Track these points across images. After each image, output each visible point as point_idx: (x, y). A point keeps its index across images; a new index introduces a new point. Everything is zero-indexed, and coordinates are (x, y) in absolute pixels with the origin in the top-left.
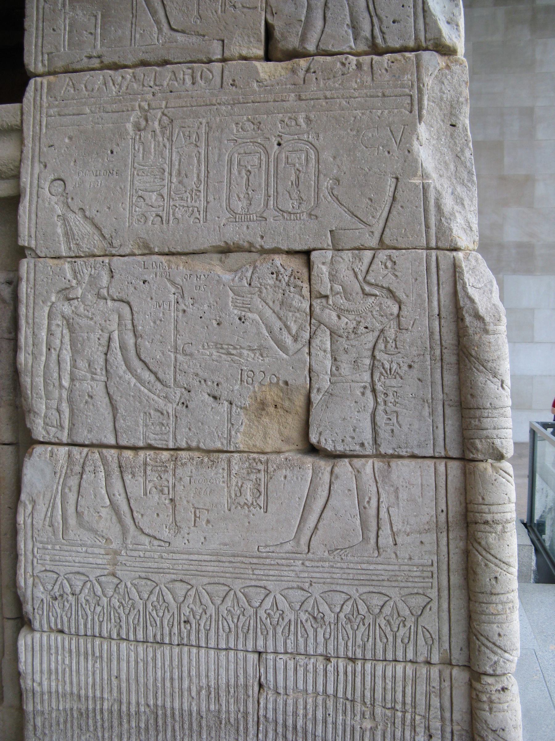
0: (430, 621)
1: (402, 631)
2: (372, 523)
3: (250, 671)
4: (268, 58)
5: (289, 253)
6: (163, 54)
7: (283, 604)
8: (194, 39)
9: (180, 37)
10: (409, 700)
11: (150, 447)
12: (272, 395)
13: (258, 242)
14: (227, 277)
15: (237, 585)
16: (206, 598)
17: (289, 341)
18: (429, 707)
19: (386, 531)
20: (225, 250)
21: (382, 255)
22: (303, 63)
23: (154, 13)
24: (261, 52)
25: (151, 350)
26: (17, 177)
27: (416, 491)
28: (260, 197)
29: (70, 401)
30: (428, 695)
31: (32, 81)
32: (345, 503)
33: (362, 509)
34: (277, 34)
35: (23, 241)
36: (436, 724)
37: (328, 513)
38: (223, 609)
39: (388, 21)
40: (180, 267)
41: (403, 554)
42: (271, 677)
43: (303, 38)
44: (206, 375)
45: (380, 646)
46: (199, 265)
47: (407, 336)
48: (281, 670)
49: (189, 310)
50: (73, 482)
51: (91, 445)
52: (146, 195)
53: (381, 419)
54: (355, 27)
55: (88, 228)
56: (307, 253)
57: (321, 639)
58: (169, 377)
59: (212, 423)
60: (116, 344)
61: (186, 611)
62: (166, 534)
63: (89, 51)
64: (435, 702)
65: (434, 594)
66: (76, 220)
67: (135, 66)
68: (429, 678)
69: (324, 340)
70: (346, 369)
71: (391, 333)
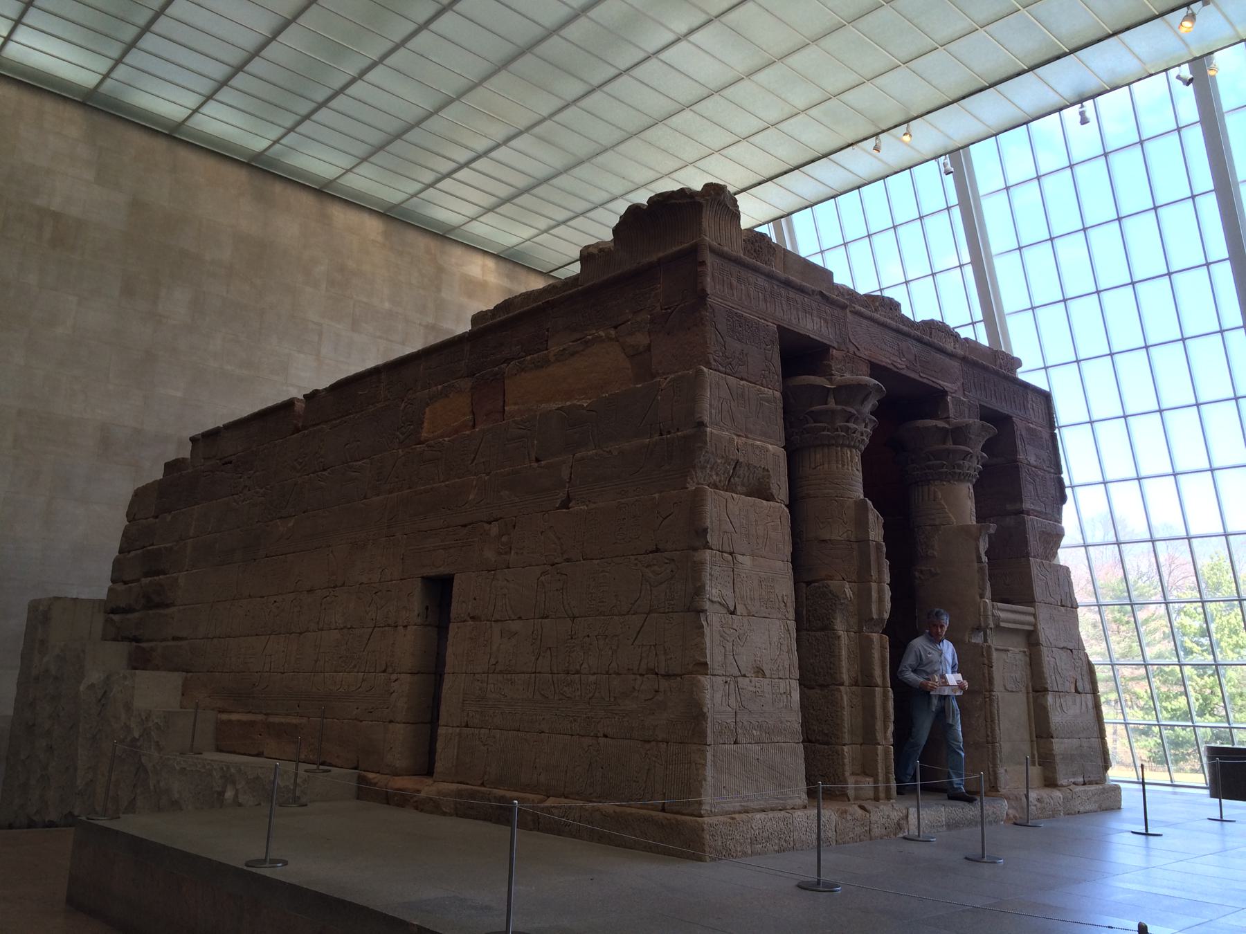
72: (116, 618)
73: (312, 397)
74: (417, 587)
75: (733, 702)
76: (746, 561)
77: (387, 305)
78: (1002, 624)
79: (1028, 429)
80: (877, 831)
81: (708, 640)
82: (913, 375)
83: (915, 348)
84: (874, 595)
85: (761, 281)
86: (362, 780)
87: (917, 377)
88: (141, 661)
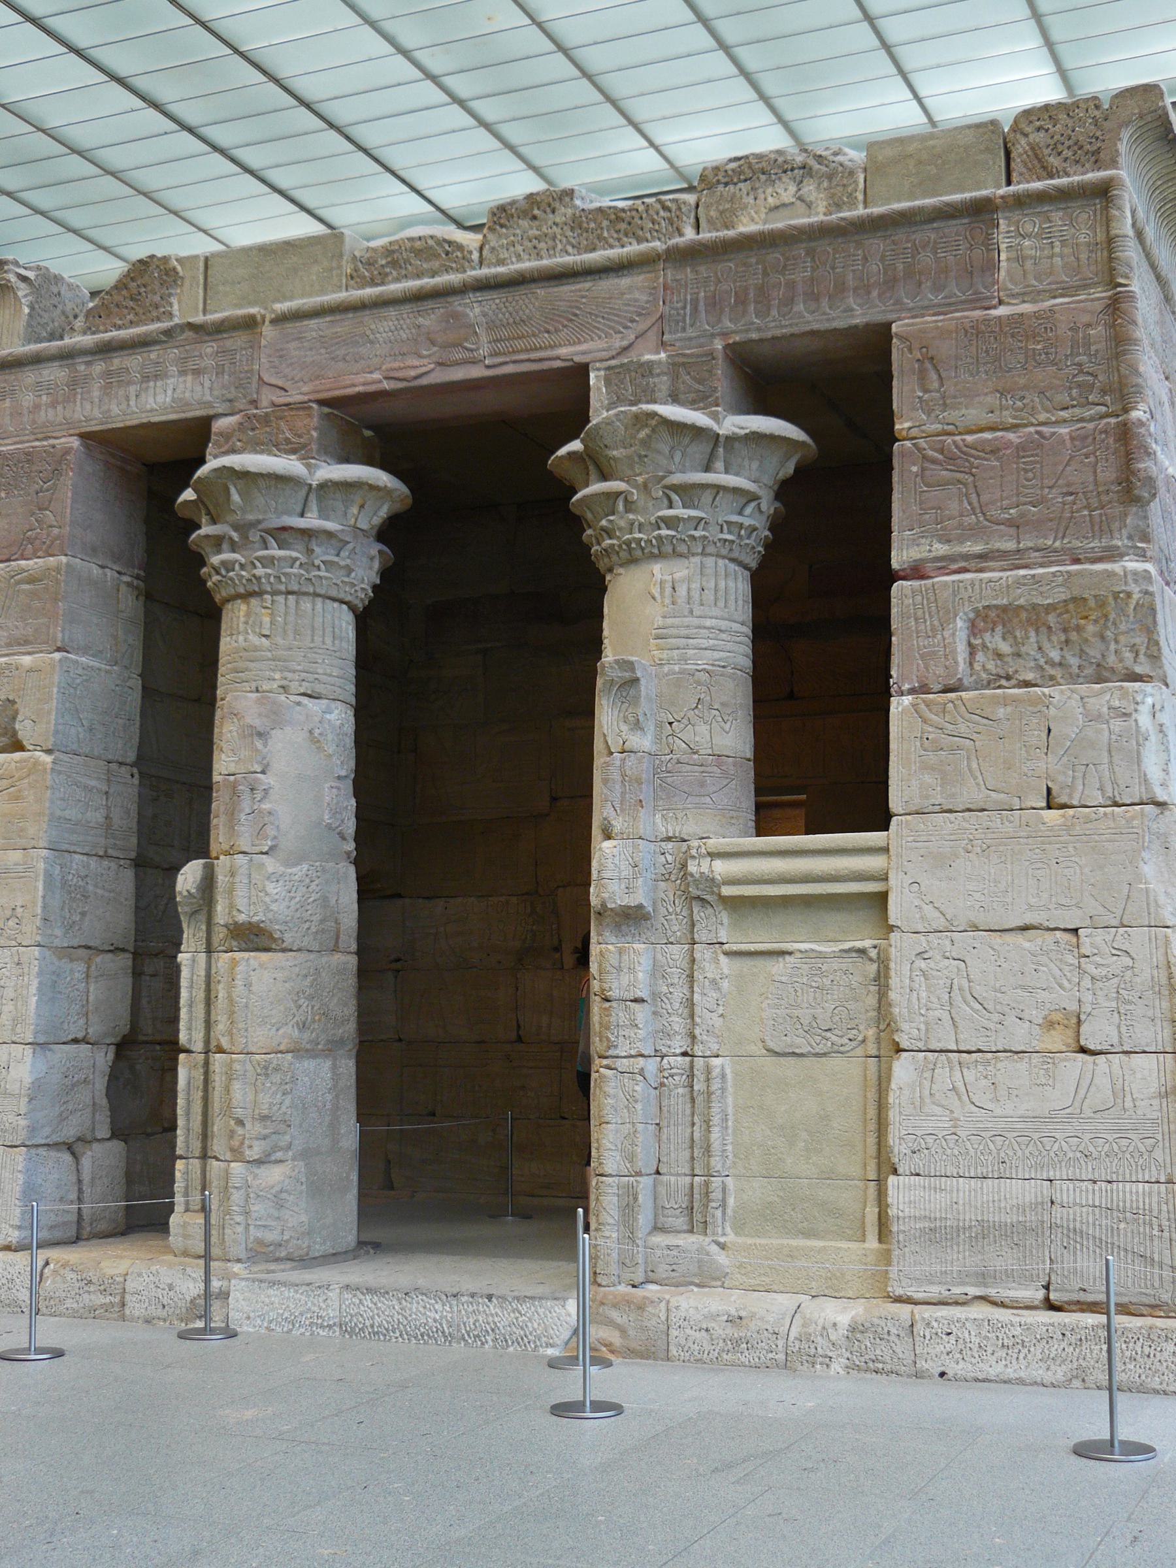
0: (1158, 1154)
1: (1141, 1161)
2: (1119, 1093)
3: (1045, 1192)
4: (1049, 807)
5: (1065, 930)
6: (981, 805)
7: (1065, 1147)
8: (1002, 795)
9: (993, 794)
10: (1147, 1207)
11: (979, 1051)
12: (1057, 1017)
13: (1046, 924)
14: (1027, 945)
15: (1036, 1136)
16: (1016, 1147)
17: (1065, 983)
18: (1160, 1211)
19: (1128, 1099)
20: (1025, 928)
21: (1121, 930)
22: (1071, 812)
23: (975, 778)
24: (1044, 804)
25: (978, 990)
26: (885, 878)
27: (1146, 1073)
28: (1045, 895)
29: (927, 1024)
30: (1159, 1203)
31: (894, 819)
32: (1103, 1082)
33: (1113, 1084)
34: (1054, 792)
35: (891, 922)
36: (1165, 1223)
37: (1093, 1089)
38: (1027, 1152)
39: (1123, 787)
40: (996, 939)
41: (1139, 1112)
42: (1058, 1195)
43: (1070, 796)
44: (1014, 1005)
45: (1127, 1171)
46: (1008, 937)
47: (1138, 980)
48: (1065, 1192)
49: (1004, 965)
50: (928, 1075)
51: (941, 1051)
52: (974, 894)
53: (1123, 1029)
54: (1101, 789)
55: (937, 914)
56: (1076, 930)
57: (1090, 1169)
58: (990, 1007)
59: (1020, 1035)
60: (955, 987)
61: (1002, 1154)
62: (990, 1106)
63: (933, 801)
64: (1164, 1207)
65: (1159, 1137)
66: (928, 909)
67: (963, 811)
68: (1159, 1193)
69: (1087, 982)
70: (1101, 1000)
71: (1127, 978)
78: (727, 891)
79: (977, 331)
80: (135, 1308)
87: (477, 372)
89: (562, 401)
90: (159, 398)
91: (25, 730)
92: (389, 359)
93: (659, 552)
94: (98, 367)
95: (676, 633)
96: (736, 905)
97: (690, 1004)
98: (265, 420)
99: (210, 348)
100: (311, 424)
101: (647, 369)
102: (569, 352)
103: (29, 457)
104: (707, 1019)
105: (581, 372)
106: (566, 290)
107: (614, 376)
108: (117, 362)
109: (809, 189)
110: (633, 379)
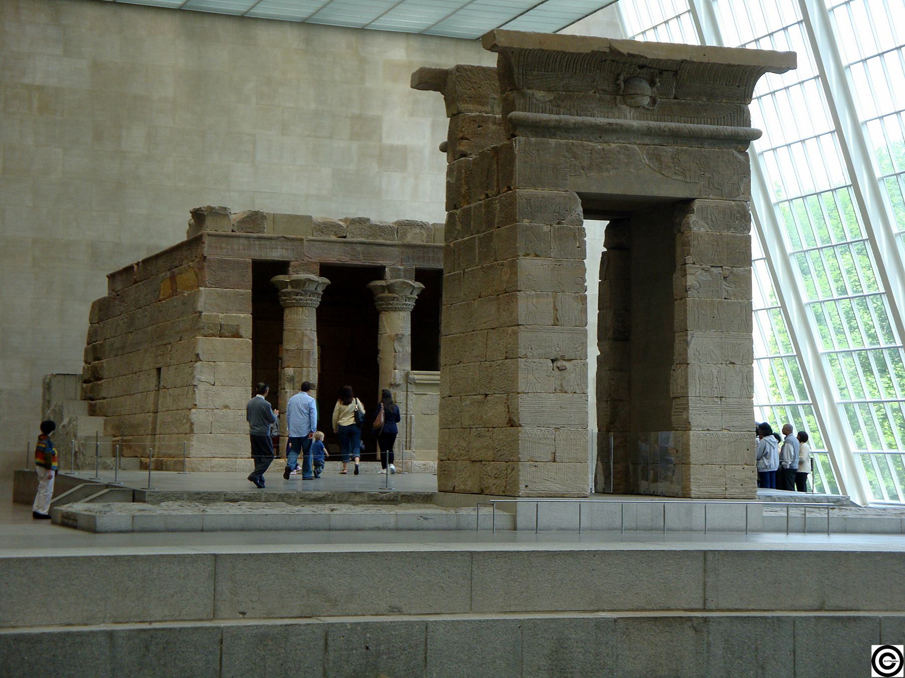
72: (85, 385)
73: (138, 264)
74: (154, 372)
75: (210, 418)
76: (223, 363)
77: (313, 106)
81: (197, 396)
82: (355, 263)
83: (359, 248)
84: (305, 373)
85: (242, 241)
86: (141, 462)
88: (93, 412)
89: (378, 272)
90: (276, 254)
91: (242, 332)
92: (337, 256)
93: (402, 310)
94: (257, 242)
95: (397, 326)
96: (416, 384)
97: (407, 404)
98: (306, 264)
99: (289, 243)
100: (317, 268)
101: (399, 269)
102: (381, 262)
103: (238, 262)
104: (410, 407)
105: (384, 267)
106: (380, 248)
107: (392, 270)
108: (263, 242)
109: (422, 231)
110: (396, 272)
